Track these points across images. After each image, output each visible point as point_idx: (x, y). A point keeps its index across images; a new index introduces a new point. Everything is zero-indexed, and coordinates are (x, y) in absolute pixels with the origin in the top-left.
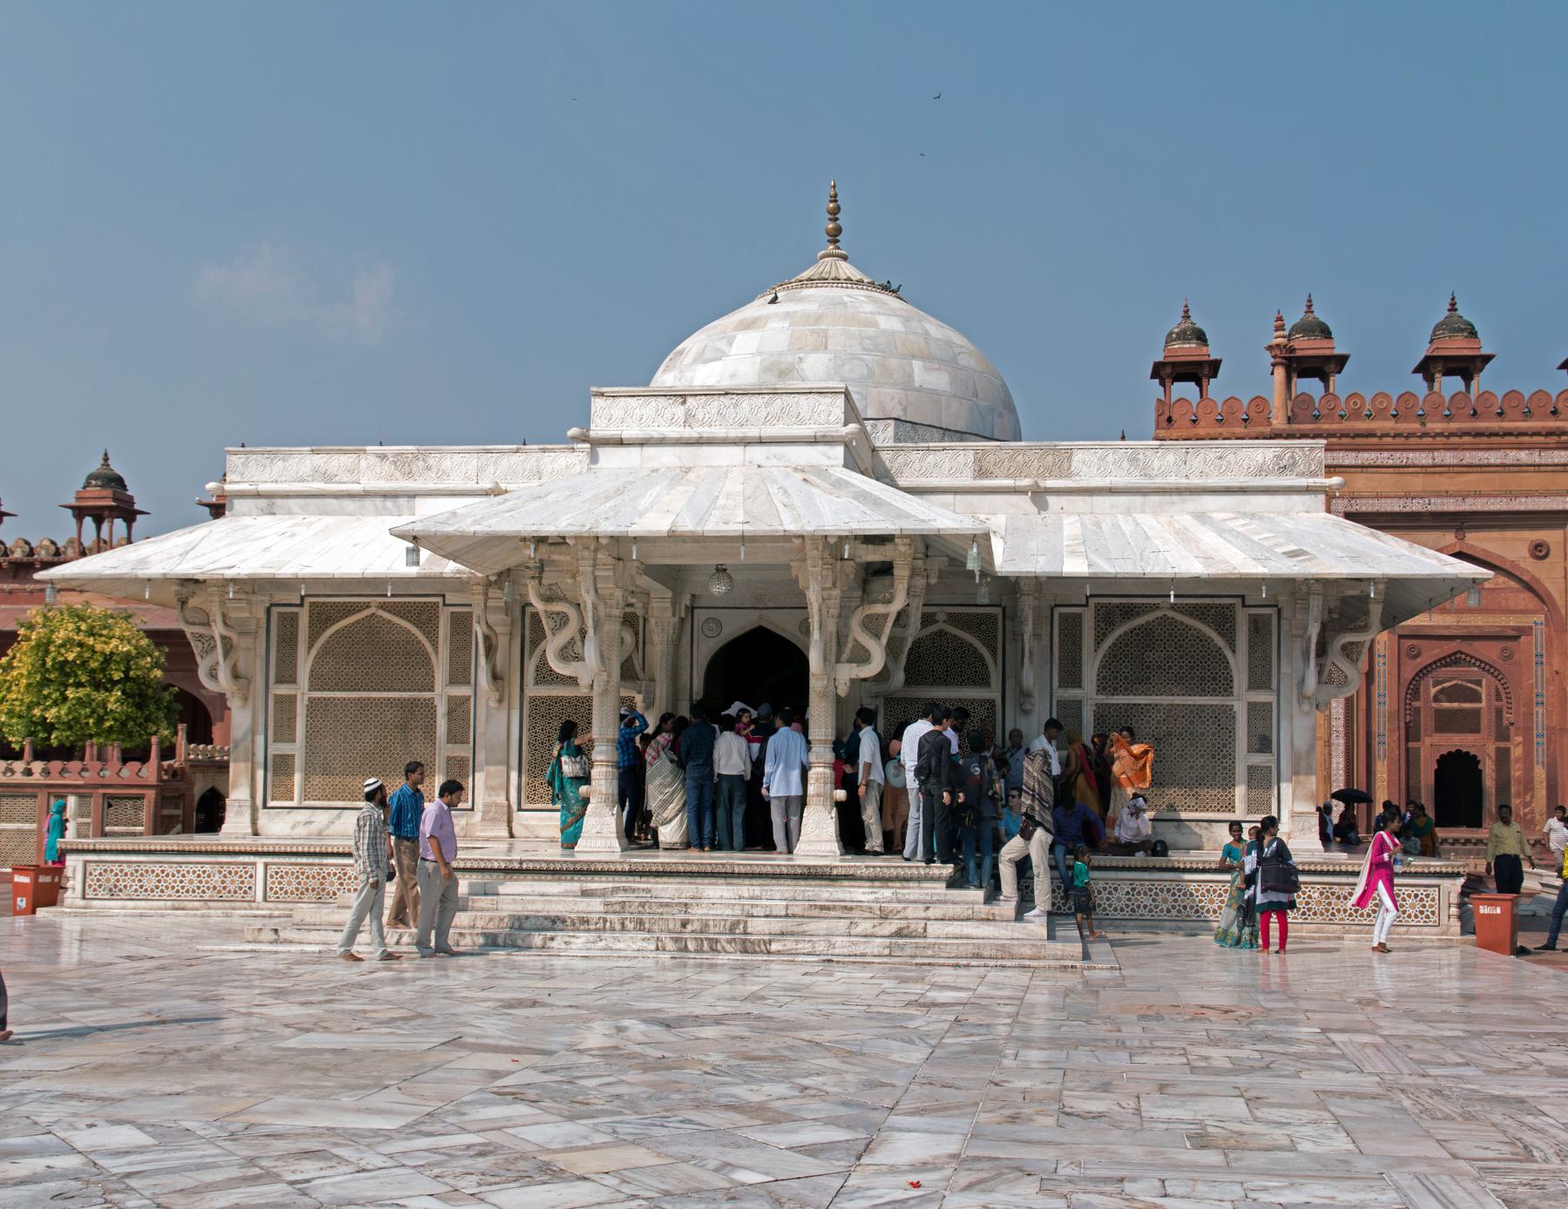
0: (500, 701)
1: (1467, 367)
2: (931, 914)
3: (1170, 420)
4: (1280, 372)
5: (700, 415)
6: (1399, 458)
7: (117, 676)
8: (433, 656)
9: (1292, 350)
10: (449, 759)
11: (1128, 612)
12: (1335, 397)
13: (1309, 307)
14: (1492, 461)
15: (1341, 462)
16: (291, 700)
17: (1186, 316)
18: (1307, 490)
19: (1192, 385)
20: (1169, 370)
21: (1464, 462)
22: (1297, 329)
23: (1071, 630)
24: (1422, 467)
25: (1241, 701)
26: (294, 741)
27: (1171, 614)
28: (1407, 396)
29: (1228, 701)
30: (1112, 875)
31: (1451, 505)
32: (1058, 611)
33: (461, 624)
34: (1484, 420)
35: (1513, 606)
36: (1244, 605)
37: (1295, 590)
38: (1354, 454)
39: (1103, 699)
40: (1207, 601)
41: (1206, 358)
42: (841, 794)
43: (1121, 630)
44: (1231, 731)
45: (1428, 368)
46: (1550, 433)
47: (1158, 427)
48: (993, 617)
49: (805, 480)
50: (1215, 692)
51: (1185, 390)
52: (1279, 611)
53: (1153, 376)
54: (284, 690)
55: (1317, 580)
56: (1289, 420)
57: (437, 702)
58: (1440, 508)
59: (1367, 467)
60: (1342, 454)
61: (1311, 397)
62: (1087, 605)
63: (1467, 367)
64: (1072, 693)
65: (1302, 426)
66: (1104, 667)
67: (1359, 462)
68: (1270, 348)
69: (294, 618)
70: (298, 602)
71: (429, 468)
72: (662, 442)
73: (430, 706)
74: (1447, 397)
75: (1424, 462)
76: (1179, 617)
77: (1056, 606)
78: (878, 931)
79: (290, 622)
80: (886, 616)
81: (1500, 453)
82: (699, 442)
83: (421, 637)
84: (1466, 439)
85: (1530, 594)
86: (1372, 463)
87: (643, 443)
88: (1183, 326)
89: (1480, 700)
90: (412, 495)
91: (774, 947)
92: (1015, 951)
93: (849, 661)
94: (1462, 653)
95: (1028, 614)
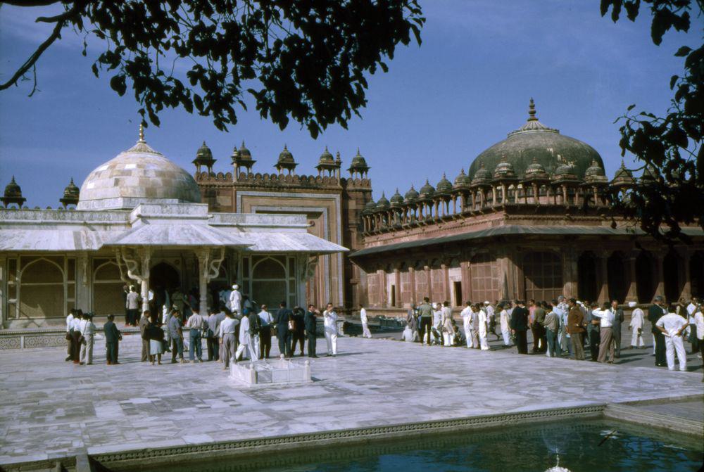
4: (235, 165)
10: (68, 302)
11: (261, 257)
23: (246, 261)
25: (287, 280)
43: (257, 263)
45: (279, 166)
50: (281, 278)
56: (238, 180)
64: (247, 279)
66: (254, 272)
68: (233, 157)
73: (61, 288)
76: (273, 259)
83: (58, 266)
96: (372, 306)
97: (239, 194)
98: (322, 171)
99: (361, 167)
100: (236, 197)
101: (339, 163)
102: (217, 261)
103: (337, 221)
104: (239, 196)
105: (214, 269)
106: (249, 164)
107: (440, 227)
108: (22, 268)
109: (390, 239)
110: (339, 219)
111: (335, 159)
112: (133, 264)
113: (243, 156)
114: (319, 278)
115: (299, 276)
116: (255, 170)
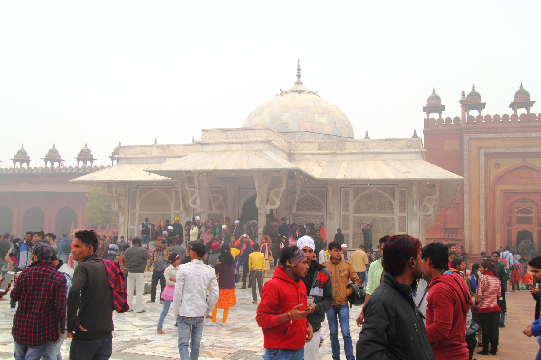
0: (187, 215)
3: (428, 125)
15: (483, 137)
17: (434, 92)
21: (525, 136)
22: (469, 95)
23: (346, 193)
24: (510, 138)
26: (134, 225)
28: (506, 116)
29: (393, 216)
31: (521, 150)
32: (342, 189)
36: (397, 187)
38: (487, 134)
39: (355, 215)
40: (387, 186)
44: (393, 225)
45: (514, 106)
47: (425, 127)
49: (256, 154)
51: (435, 116)
52: (408, 189)
54: (133, 211)
55: (415, 180)
57: (171, 215)
59: (493, 138)
62: (351, 187)
64: (346, 213)
68: (460, 101)
70: (137, 187)
72: (219, 143)
77: (342, 187)
80: (280, 192)
82: (229, 143)
86: (494, 137)
87: (215, 144)
88: (433, 95)
89: (531, 213)
90: (165, 158)
93: (270, 204)
94: (525, 198)
97: (466, 137)
105: (275, 199)
112: (194, 192)
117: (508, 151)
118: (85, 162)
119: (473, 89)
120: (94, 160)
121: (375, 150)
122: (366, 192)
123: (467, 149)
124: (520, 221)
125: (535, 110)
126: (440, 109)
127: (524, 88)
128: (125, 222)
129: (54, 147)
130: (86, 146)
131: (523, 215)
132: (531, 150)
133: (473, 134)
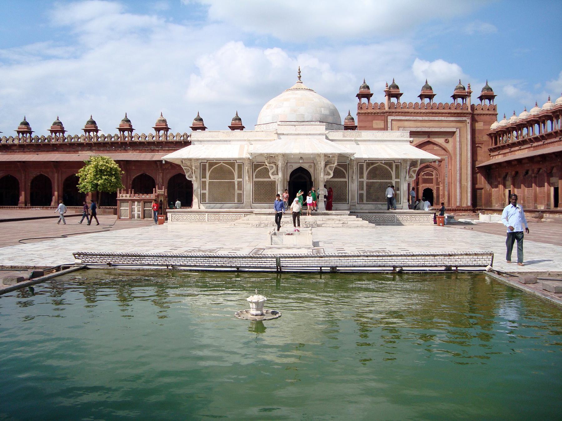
1: (431, 97)
2: (348, 220)
3: (361, 108)
4: (387, 97)
5: (298, 129)
6: (415, 118)
7: (113, 173)
8: (234, 173)
9: (390, 92)
10: (238, 193)
11: (372, 164)
12: (400, 103)
13: (394, 81)
14: (436, 119)
16: (205, 182)
17: (364, 83)
18: (407, 141)
19: (366, 99)
20: (361, 96)
23: (361, 167)
25: (394, 181)
27: (381, 164)
28: (416, 103)
30: (372, 214)
31: (427, 130)
33: (240, 167)
34: (435, 109)
35: (441, 154)
37: (405, 160)
38: (404, 117)
39: (368, 181)
41: (369, 93)
42: (325, 200)
45: (422, 97)
46: (449, 113)
47: (358, 109)
48: (347, 165)
51: (364, 100)
53: (356, 97)
54: (204, 180)
56: (389, 108)
58: (424, 130)
60: (402, 117)
61: (394, 103)
63: (431, 97)
64: (362, 180)
65: (392, 110)
66: (368, 174)
67: (406, 119)
68: (385, 91)
69: (205, 165)
71: (233, 135)
72: (291, 134)
73: (234, 182)
74: (426, 103)
75: (421, 119)
76: (382, 165)
78: (339, 223)
79: (204, 166)
81: (438, 117)
82: (298, 134)
84: (430, 114)
85: (444, 151)
87: (287, 134)
88: (364, 85)
89: (433, 176)
90: (230, 141)
91: (323, 226)
92: (364, 226)
95: (355, 164)
96: (495, 206)
98: (456, 100)
99: (488, 96)
100: (387, 121)
101: (470, 93)
102: (332, 165)
103: (467, 139)
104: (389, 120)
106: (398, 96)
107: (544, 142)
108: (209, 171)
109: (508, 153)
110: (469, 137)
111: (467, 90)
112: (273, 166)
113: (392, 90)
114: (452, 183)
115: (402, 179)
116: (402, 99)
117: (418, 130)
118: (56, 133)
119: (394, 82)
120: (65, 132)
121: (380, 139)
122: (375, 165)
123: (390, 128)
124: (426, 181)
125: (436, 100)
126: (368, 96)
127: (428, 84)
128: (198, 188)
129: (25, 120)
130: (58, 119)
131: (428, 177)
132: (433, 130)
133: (394, 116)
